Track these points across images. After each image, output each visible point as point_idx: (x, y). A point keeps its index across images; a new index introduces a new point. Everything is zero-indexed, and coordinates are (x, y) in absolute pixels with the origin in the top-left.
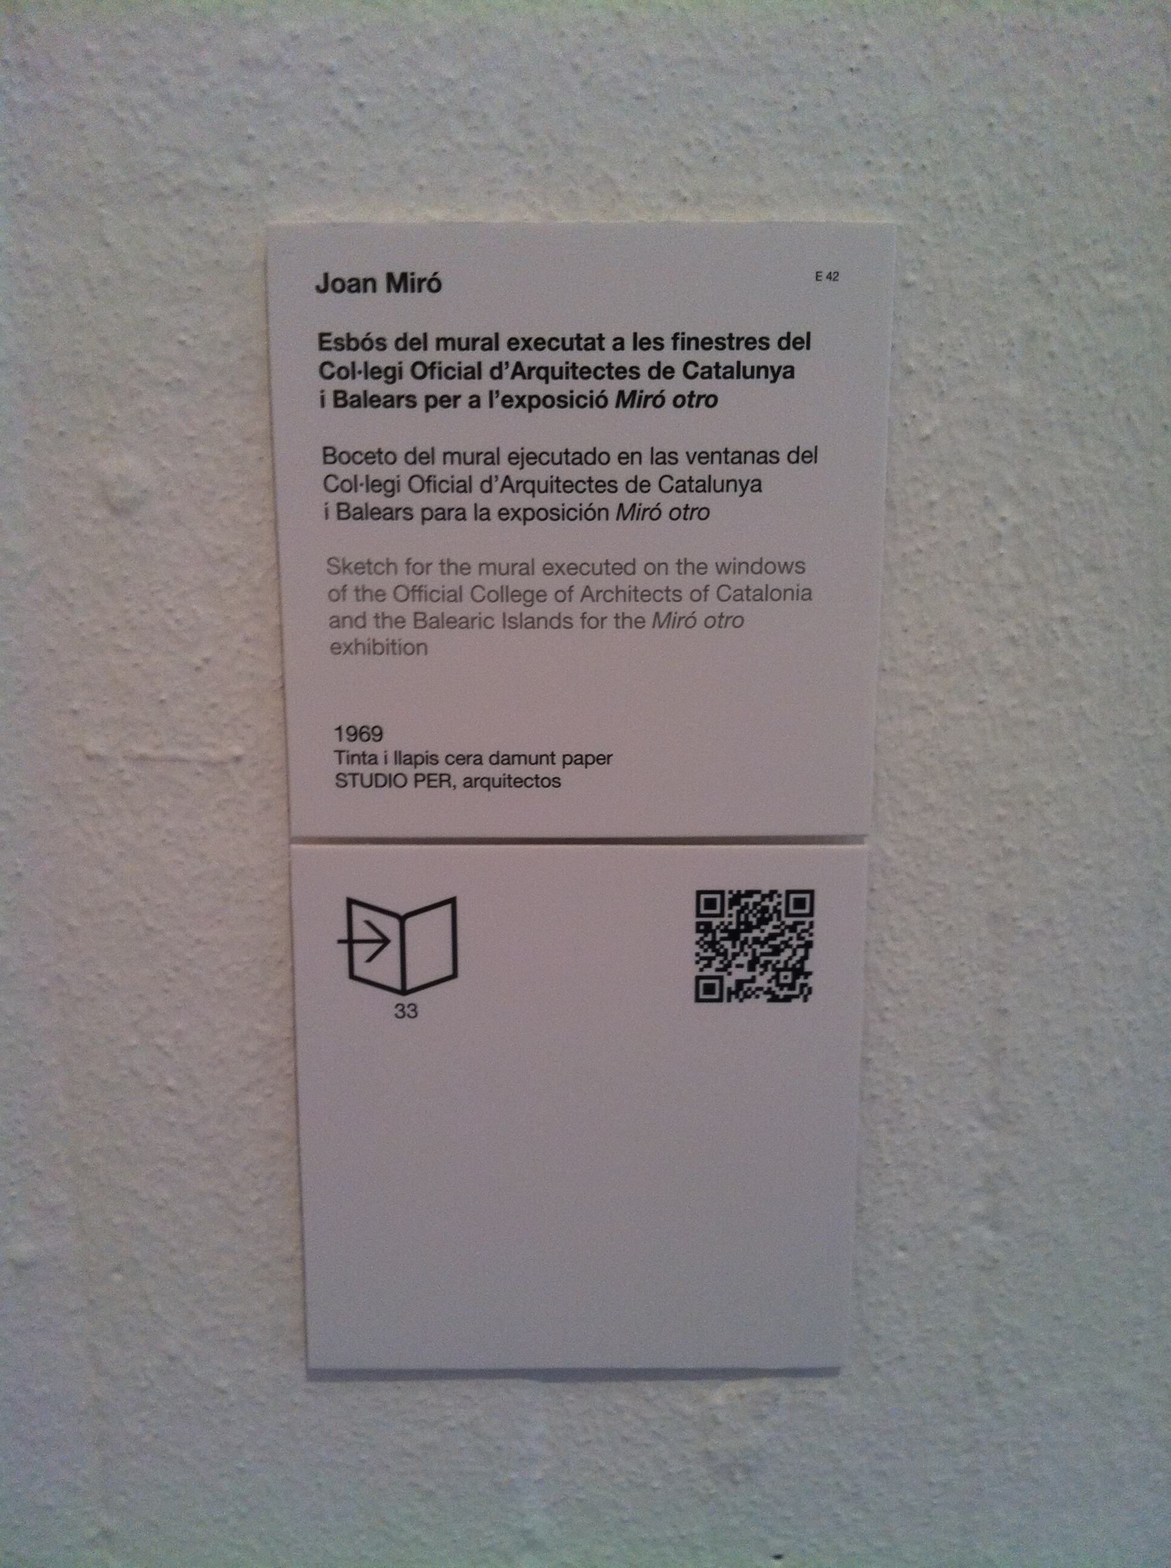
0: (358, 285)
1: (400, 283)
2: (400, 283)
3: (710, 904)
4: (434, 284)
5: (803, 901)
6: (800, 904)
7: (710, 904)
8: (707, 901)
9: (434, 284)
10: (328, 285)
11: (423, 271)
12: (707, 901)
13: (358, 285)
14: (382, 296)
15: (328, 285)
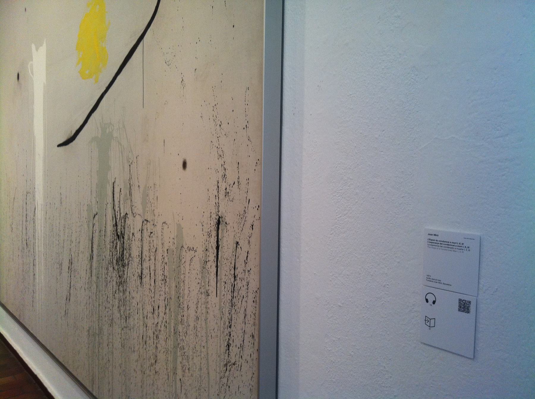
0: (431, 235)
1: (435, 235)
2: (435, 235)
3: (460, 300)
4: (438, 235)
5: (470, 302)
6: (470, 302)
7: (460, 300)
8: (460, 300)
9: (438, 235)
10: (429, 234)
11: (437, 234)
12: (460, 300)
13: (431, 235)
14: (433, 236)
15: (429, 234)
